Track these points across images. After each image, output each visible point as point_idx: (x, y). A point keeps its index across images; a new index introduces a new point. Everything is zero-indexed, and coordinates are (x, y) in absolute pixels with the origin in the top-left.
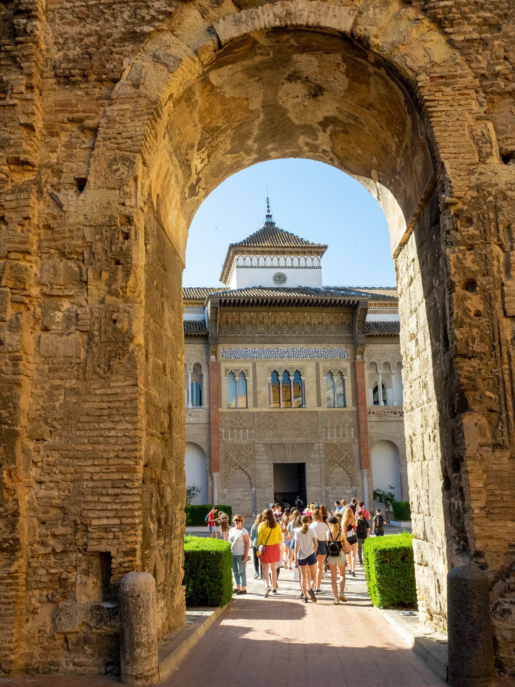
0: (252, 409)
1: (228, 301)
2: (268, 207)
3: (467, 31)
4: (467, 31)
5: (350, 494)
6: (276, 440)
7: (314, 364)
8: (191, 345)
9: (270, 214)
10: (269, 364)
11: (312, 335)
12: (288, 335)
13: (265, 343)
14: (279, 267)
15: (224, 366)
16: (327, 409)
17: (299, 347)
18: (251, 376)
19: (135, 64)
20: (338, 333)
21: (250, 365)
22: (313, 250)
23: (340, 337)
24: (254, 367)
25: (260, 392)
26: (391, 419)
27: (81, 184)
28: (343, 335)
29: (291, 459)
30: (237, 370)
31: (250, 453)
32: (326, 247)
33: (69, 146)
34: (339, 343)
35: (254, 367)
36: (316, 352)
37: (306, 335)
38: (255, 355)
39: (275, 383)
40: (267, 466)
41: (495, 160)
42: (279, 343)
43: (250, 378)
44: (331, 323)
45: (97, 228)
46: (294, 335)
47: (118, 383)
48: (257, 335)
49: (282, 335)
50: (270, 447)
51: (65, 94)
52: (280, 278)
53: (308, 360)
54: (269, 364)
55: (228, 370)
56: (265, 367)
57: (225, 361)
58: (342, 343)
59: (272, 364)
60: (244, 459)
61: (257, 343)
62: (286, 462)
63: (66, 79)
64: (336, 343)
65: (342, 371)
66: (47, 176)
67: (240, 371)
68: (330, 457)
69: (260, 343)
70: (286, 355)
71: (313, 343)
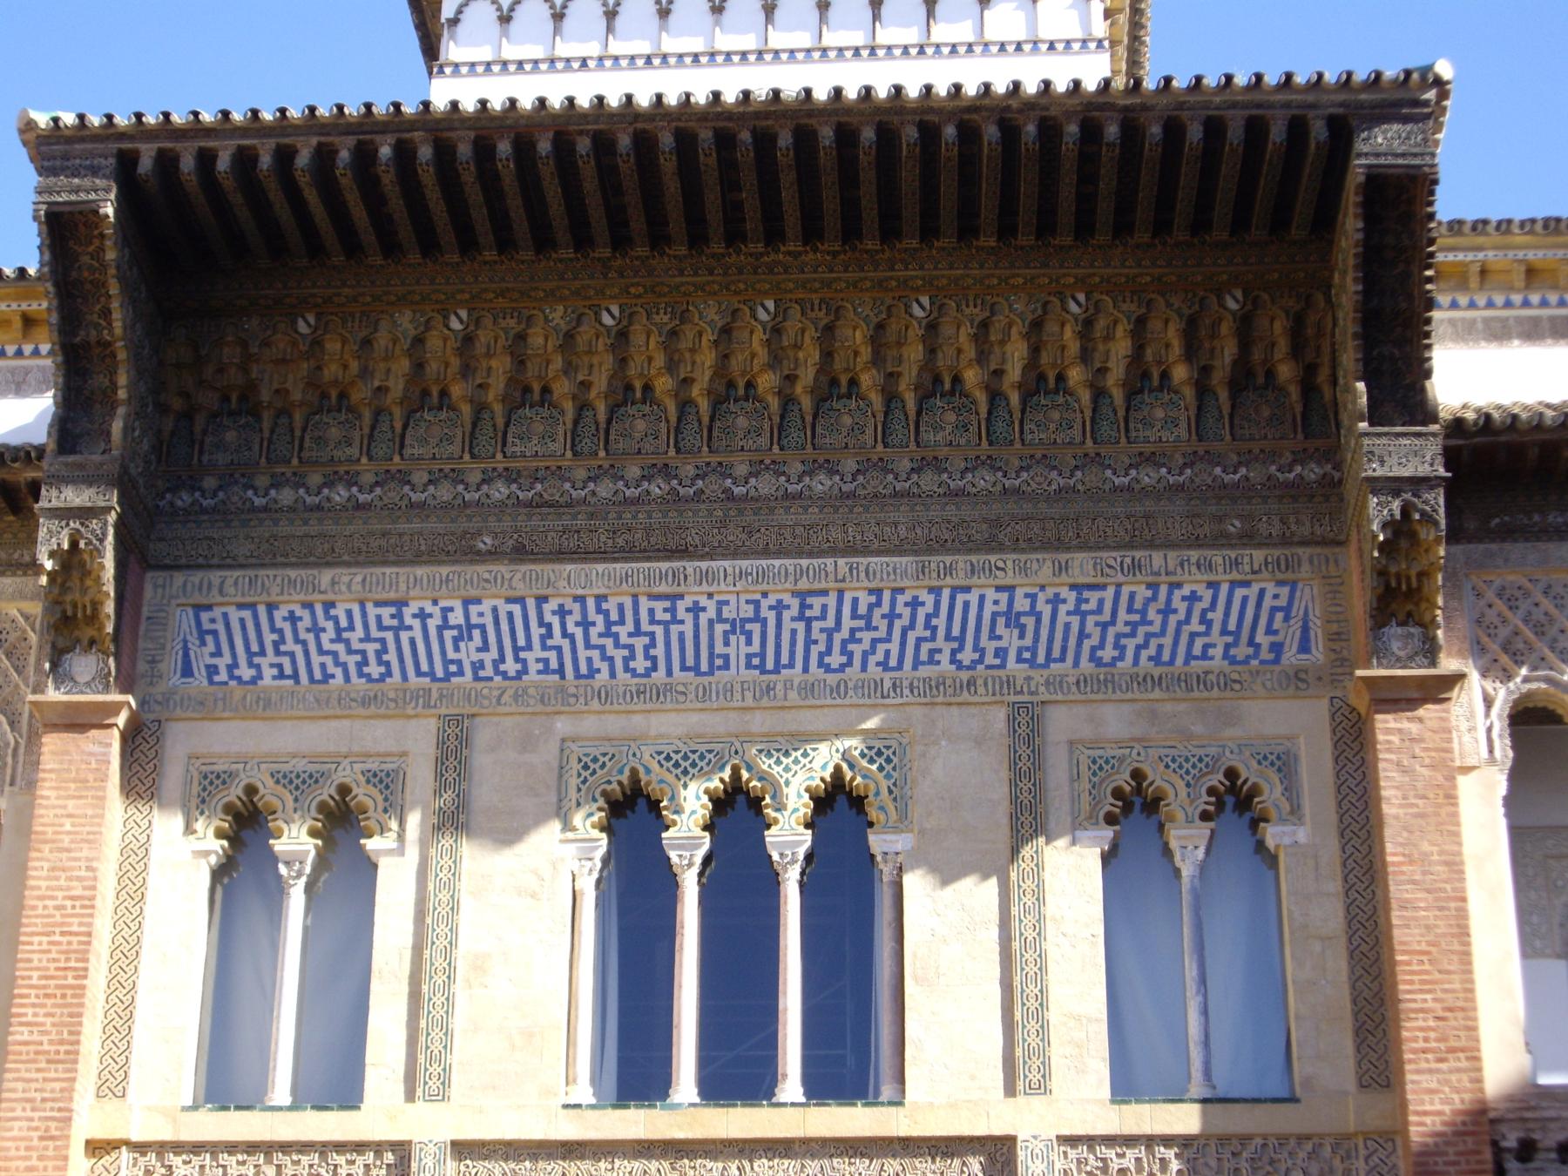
1: (188, 163)
7: (1000, 715)
10: (590, 725)
11: (984, 480)
12: (765, 485)
13: (560, 555)
17: (852, 582)
20: (1211, 458)
23: (1222, 492)
28: (1255, 474)
30: (297, 783)
34: (1220, 540)
36: (1012, 618)
37: (928, 481)
38: (468, 653)
42: (683, 552)
44: (1143, 380)
46: (821, 484)
48: (499, 491)
49: (712, 486)
53: (940, 683)
54: (590, 725)
56: (547, 753)
57: (206, 709)
58: (1248, 538)
59: (613, 724)
61: (493, 555)
64: (1197, 543)
65: (1250, 774)
69: (521, 553)
70: (738, 649)
71: (991, 544)
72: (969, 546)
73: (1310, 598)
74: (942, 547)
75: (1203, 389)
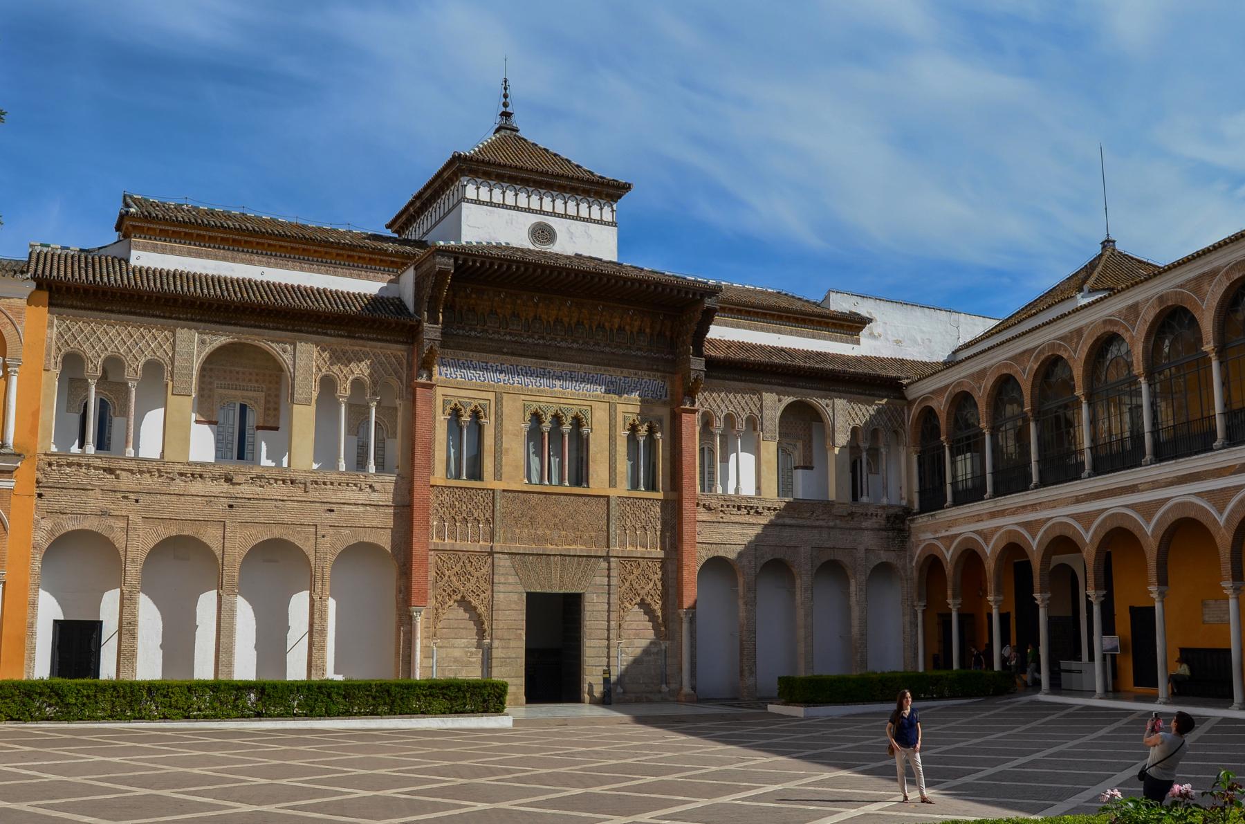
2: (506, 96)
5: (657, 653)
6: (534, 548)
8: (379, 344)
9: (508, 110)
10: (528, 398)
11: (607, 349)
12: (563, 344)
13: (521, 356)
14: (541, 212)
15: (439, 391)
16: (627, 494)
18: (493, 418)
21: (491, 396)
22: (606, 190)
24: (499, 402)
25: (507, 450)
26: (734, 519)
31: (484, 571)
32: (626, 187)
34: (652, 370)
37: (597, 348)
39: (535, 434)
40: (515, 597)
44: (641, 331)
46: (575, 346)
48: (508, 338)
49: (553, 343)
52: (543, 233)
54: (528, 398)
55: (450, 402)
58: (657, 370)
60: (473, 581)
62: (549, 591)
67: (473, 407)
68: (627, 584)
69: (513, 354)
72: (604, 365)
73: (667, 385)
74: (598, 364)
75: (652, 335)
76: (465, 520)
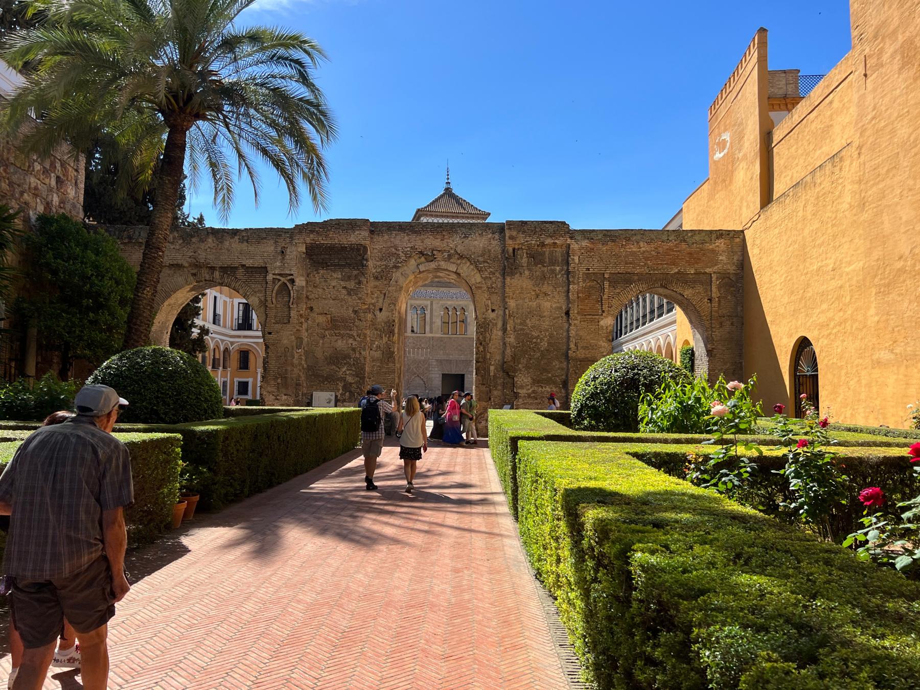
0: (428, 335)
3: (486, 274)
4: (486, 274)
6: (445, 357)
19: (396, 275)
21: (429, 303)
24: (432, 304)
27: (381, 310)
29: (454, 371)
33: (377, 298)
35: (432, 304)
41: (490, 311)
43: (428, 312)
45: (385, 323)
47: (391, 365)
50: (440, 362)
51: (377, 283)
63: (376, 278)
66: (371, 306)
76: (418, 349)
